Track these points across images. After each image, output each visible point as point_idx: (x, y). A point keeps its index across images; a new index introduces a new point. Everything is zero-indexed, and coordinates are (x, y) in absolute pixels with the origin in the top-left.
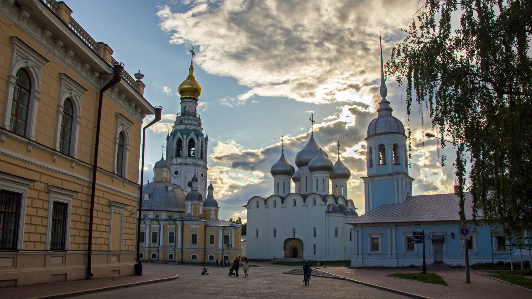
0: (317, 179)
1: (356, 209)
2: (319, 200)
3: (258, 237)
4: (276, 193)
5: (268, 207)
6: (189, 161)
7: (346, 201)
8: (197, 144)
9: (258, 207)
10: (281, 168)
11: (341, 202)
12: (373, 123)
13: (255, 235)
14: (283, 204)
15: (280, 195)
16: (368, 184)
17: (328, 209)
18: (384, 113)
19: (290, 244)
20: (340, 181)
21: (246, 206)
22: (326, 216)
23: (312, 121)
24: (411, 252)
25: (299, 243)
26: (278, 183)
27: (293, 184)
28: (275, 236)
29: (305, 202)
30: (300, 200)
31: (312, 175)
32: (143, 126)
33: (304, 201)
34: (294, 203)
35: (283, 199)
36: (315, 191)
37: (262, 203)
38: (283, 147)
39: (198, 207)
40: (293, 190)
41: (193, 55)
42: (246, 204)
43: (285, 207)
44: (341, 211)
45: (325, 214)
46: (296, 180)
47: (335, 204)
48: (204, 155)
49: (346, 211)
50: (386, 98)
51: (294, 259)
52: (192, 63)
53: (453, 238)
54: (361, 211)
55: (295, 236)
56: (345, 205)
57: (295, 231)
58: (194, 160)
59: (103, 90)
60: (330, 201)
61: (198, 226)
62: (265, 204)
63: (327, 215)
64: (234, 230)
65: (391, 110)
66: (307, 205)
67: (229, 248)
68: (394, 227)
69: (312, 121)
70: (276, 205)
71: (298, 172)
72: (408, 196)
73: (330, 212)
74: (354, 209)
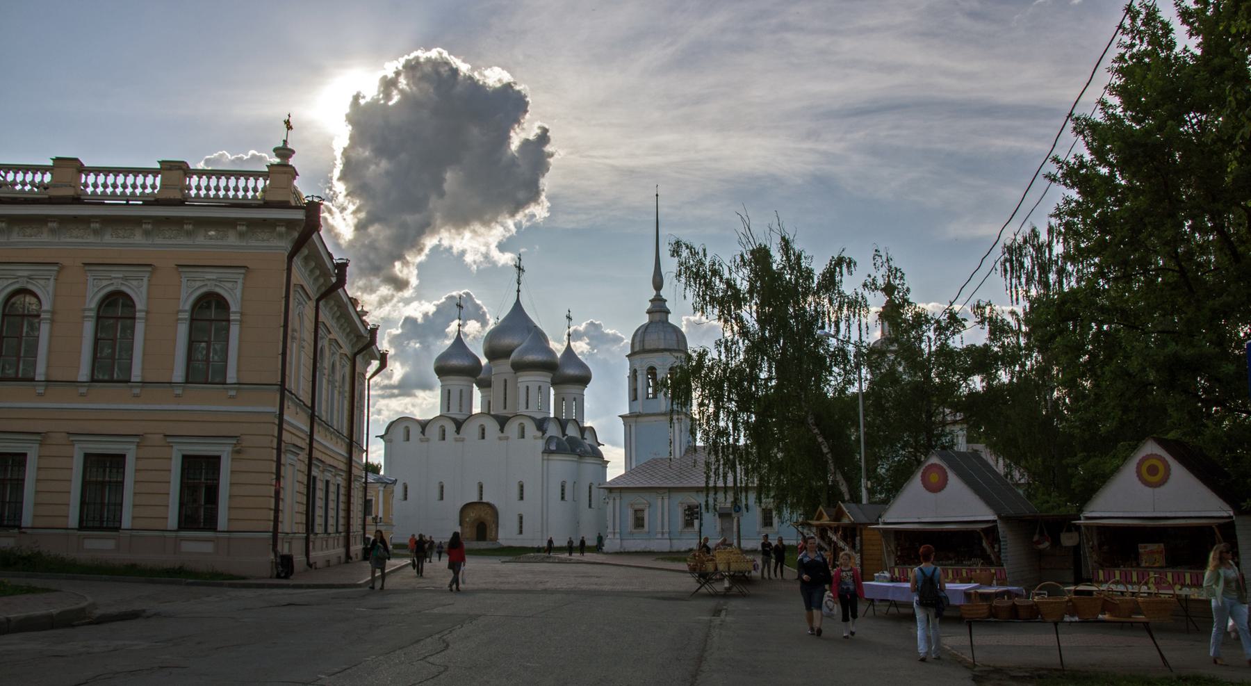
0: (528, 387)
1: (599, 445)
2: (531, 429)
3: (406, 499)
4: (445, 412)
5: (428, 440)
7: (583, 430)
10: (455, 362)
11: (572, 431)
12: (640, 332)
14: (458, 433)
15: (453, 416)
16: (630, 426)
18: (657, 317)
19: (472, 515)
20: (571, 390)
21: (382, 437)
22: (543, 460)
24: (690, 529)
27: (477, 394)
28: (442, 498)
29: (502, 432)
30: (492, 426)
31: (517, 378)
32: (367, 377)
33: (502, 430)
34: (481, 433)
35: (459, 425)
36: (522, 409)
37: (415, 431)
40: (477, 409)
41: (288, 129)
42: (383, 433)
43: (463, 440)
44: (572, 451)
45: (543, 456)
46: (485, 385)
47: (560, 436)
50: (662, 293)
51: (480, 543)
53: (747, 511)
54: (616, 468)
55: (481, 498)
56: (580, 437)
57: (481, 487)
59: (355, 355)
60: (553, 430)
62: (423, 432)
63: (545, 458)
64: (382, 488)
65: (668, 312)
67: (376, 523)
68: (667, 494)
70: (444, 435)
71: (489, 369)
72: (689, 446)
73: (552, 452)
74: (596, 445)
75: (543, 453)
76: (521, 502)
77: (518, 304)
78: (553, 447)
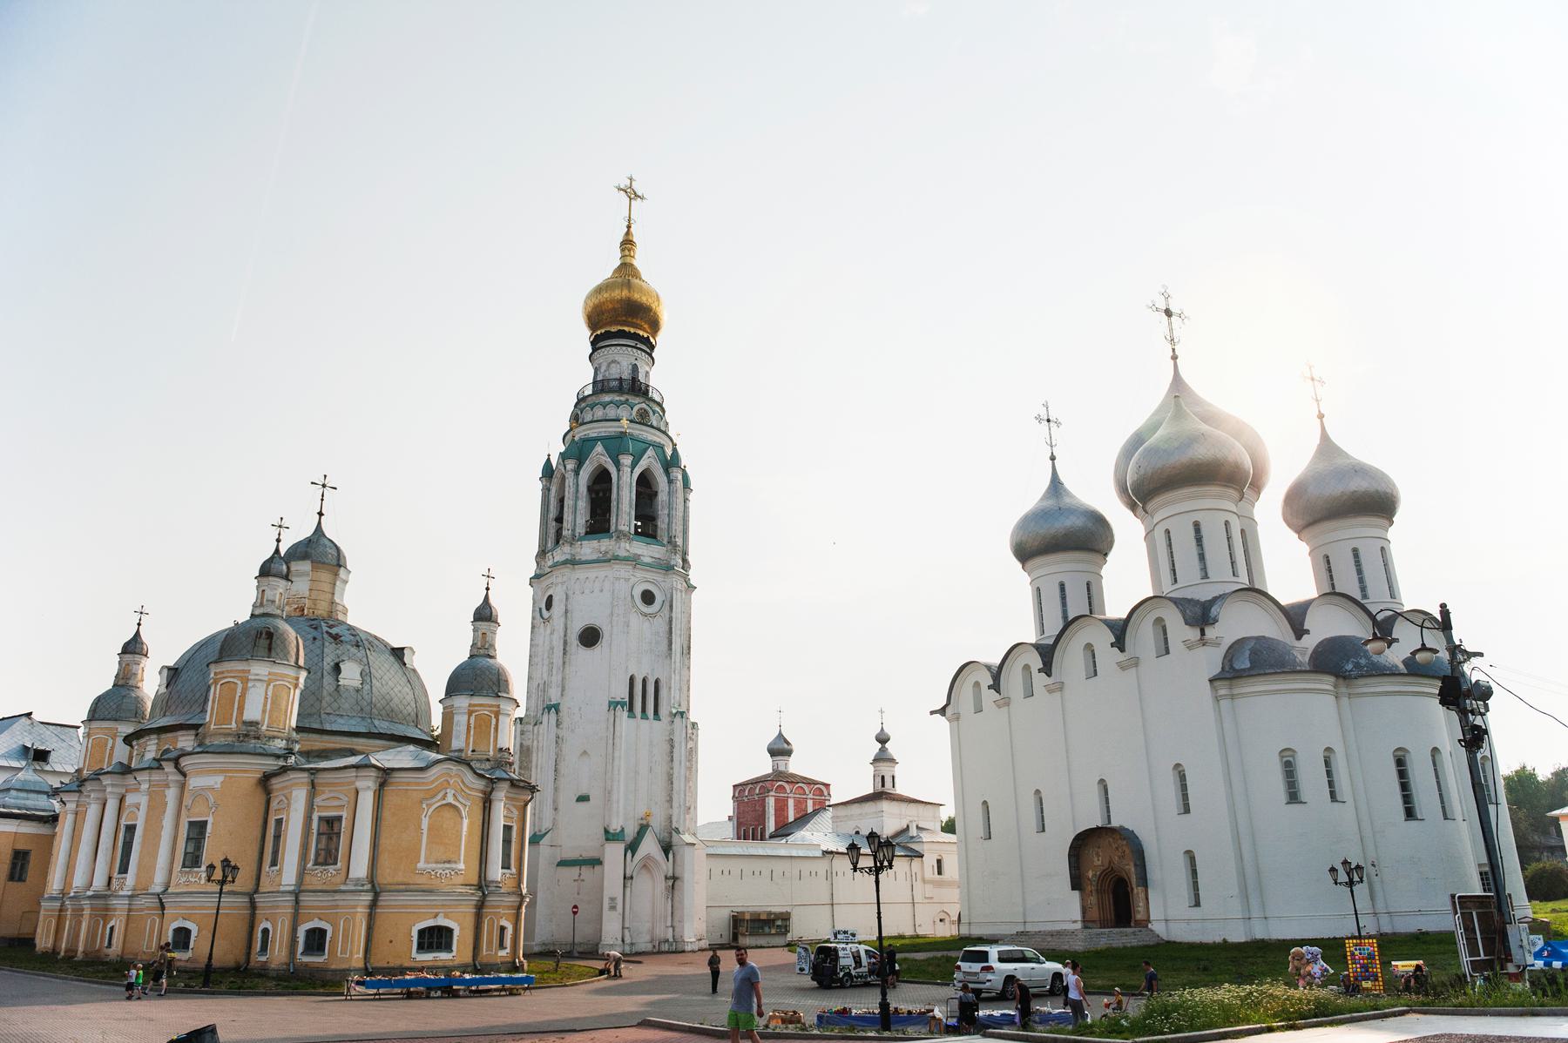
0: (1168, 532)
6: (588, 549)
8: (616, 483)
9: (979, 710)
13: (981, 832)
17: (1231, 661)
19: (1096, 861)
21: (942, 711)
22: (1217, 699)
23: (1168, 313)
26: (1038, 589)
38: (1052, 446)
39: (240, 686)
45: (1214, 689)
48: (662, 524)
49: (1357, 665)
52: (629, 227)
58: (605, 544)
61: (216, 781)
62: (996, 686)
63: (1222, 692)
66: (1135, 662)
69: (1168, 313)
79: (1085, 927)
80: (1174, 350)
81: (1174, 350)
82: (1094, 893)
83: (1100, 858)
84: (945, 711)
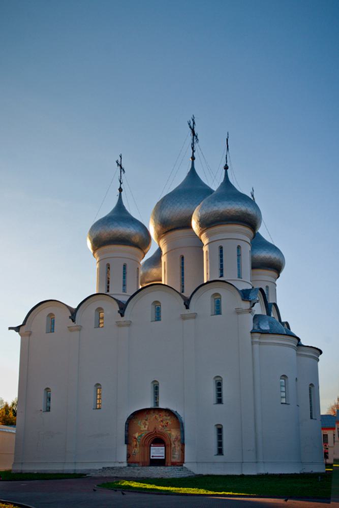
0: (221, 249)
9: (51, 329)
13: (42, 406)
19: (143, 427)
21: (17, 329)
22: (253, 343)
23: (194, 134)
25: (170, 423)
30: (171, 306)
38: (121, 183)
45: (252, 338)
55: (157, 403)
75: (251, 333)
76: (220, 406)
77: (193, 172)
78: (265, 327)
79: (129, 466)
80: (193, 154)
81: (193, 154)
82: (138, 446)
83: (147, 426)
84: (19, 329)
